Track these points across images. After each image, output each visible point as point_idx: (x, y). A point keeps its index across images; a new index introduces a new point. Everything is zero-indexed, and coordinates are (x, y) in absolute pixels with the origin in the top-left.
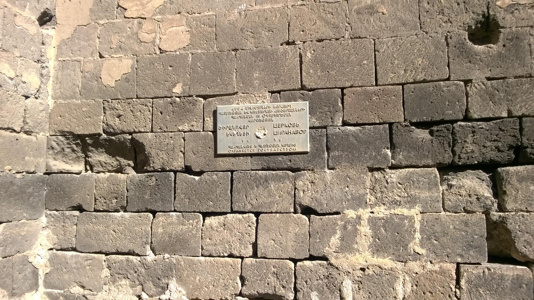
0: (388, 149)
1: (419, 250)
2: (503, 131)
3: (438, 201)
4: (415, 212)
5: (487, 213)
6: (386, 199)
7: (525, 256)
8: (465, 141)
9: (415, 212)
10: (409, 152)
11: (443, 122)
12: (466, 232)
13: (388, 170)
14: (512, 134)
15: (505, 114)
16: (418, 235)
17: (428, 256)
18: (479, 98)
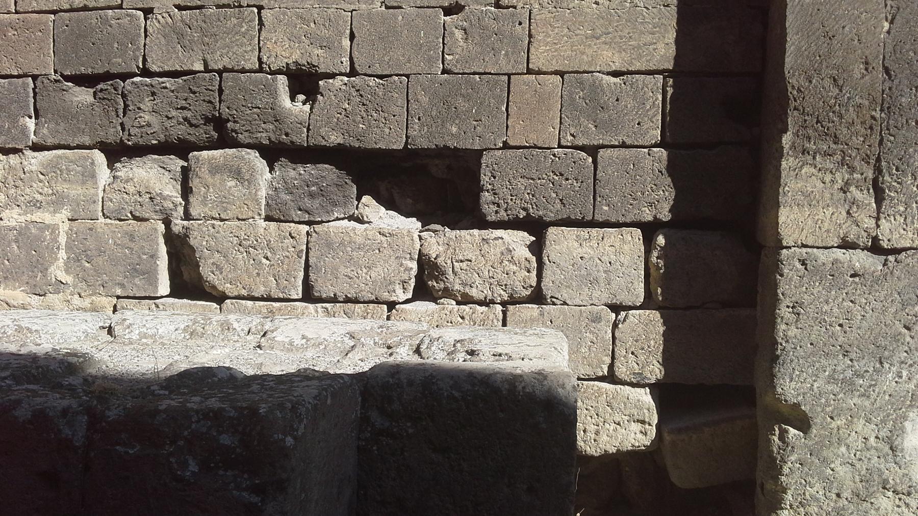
0: (30, 117)
1: (63, 277)
2: (194, 93)
3: (95, 202)
4: (60, 219)
5: (167, 222)
6: (22, 199)
7: (214, 287)
8: (139, 108)
9: (60, 219)
10: (57, 124)
11: (107, 76)
12: (131, 249)
13: (28, 153)
14: (207, 98)
15: (199, 66)
16: (62, 254)
17: (75, 286)
18: (163, 41)
